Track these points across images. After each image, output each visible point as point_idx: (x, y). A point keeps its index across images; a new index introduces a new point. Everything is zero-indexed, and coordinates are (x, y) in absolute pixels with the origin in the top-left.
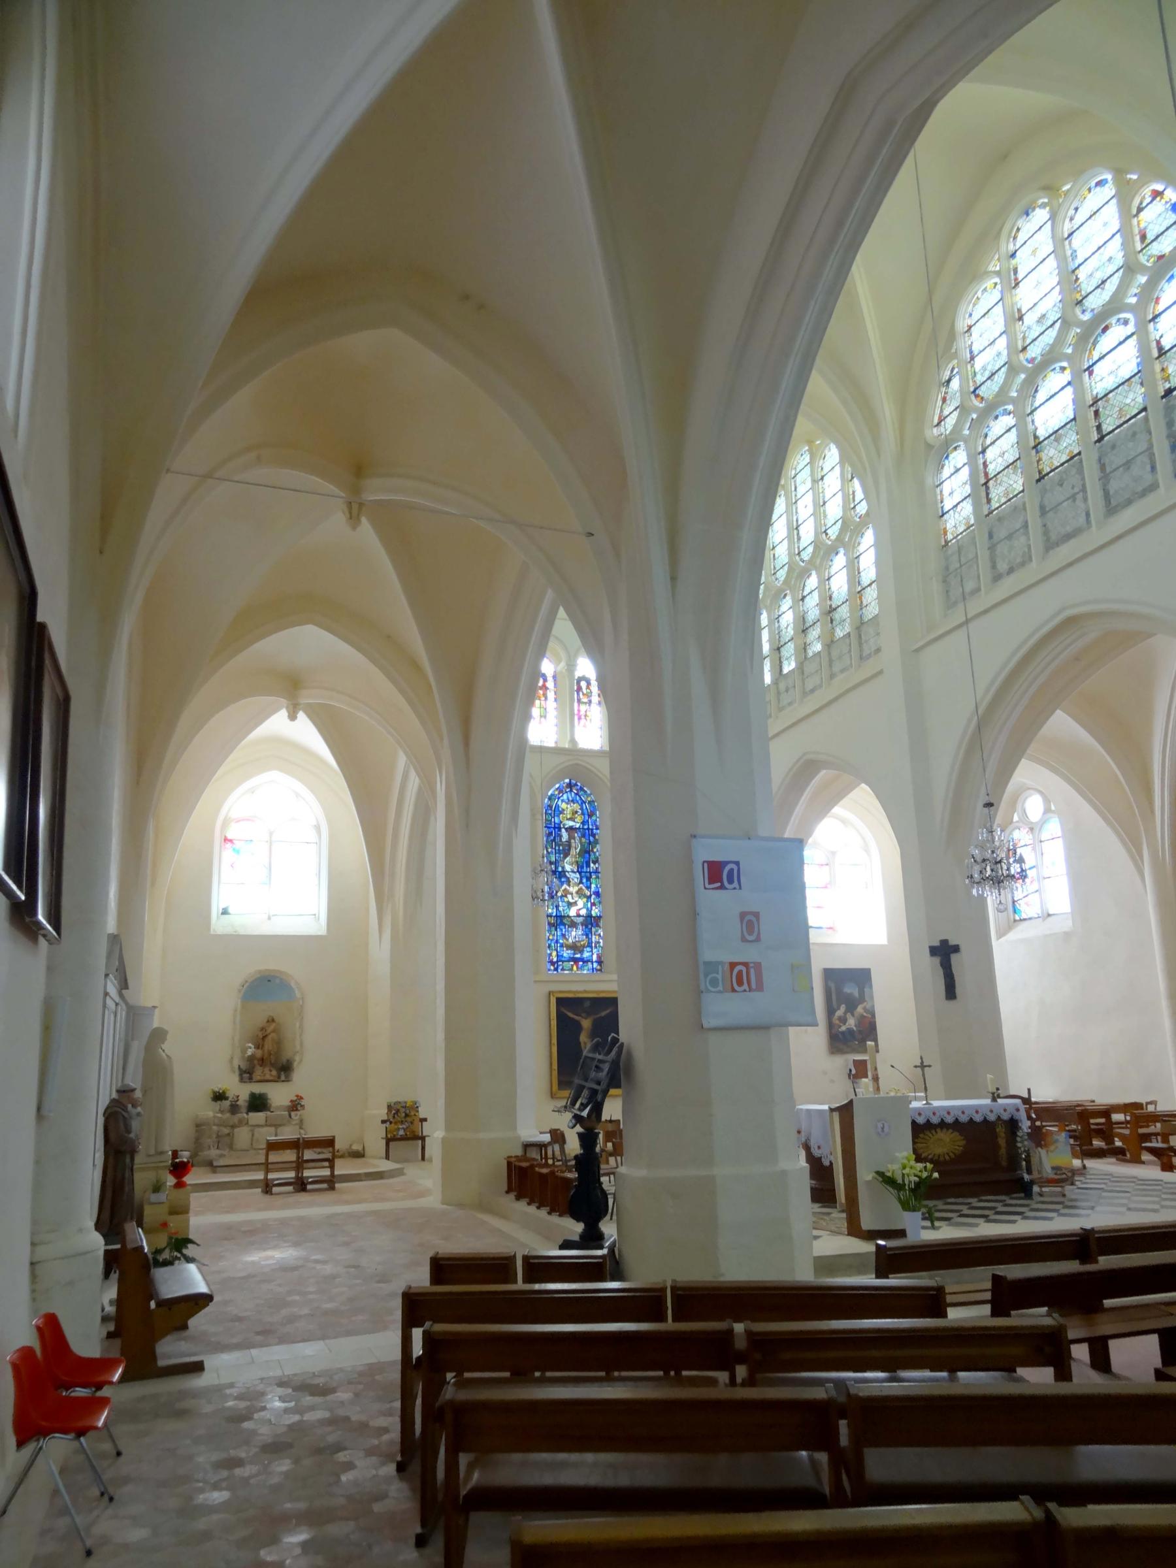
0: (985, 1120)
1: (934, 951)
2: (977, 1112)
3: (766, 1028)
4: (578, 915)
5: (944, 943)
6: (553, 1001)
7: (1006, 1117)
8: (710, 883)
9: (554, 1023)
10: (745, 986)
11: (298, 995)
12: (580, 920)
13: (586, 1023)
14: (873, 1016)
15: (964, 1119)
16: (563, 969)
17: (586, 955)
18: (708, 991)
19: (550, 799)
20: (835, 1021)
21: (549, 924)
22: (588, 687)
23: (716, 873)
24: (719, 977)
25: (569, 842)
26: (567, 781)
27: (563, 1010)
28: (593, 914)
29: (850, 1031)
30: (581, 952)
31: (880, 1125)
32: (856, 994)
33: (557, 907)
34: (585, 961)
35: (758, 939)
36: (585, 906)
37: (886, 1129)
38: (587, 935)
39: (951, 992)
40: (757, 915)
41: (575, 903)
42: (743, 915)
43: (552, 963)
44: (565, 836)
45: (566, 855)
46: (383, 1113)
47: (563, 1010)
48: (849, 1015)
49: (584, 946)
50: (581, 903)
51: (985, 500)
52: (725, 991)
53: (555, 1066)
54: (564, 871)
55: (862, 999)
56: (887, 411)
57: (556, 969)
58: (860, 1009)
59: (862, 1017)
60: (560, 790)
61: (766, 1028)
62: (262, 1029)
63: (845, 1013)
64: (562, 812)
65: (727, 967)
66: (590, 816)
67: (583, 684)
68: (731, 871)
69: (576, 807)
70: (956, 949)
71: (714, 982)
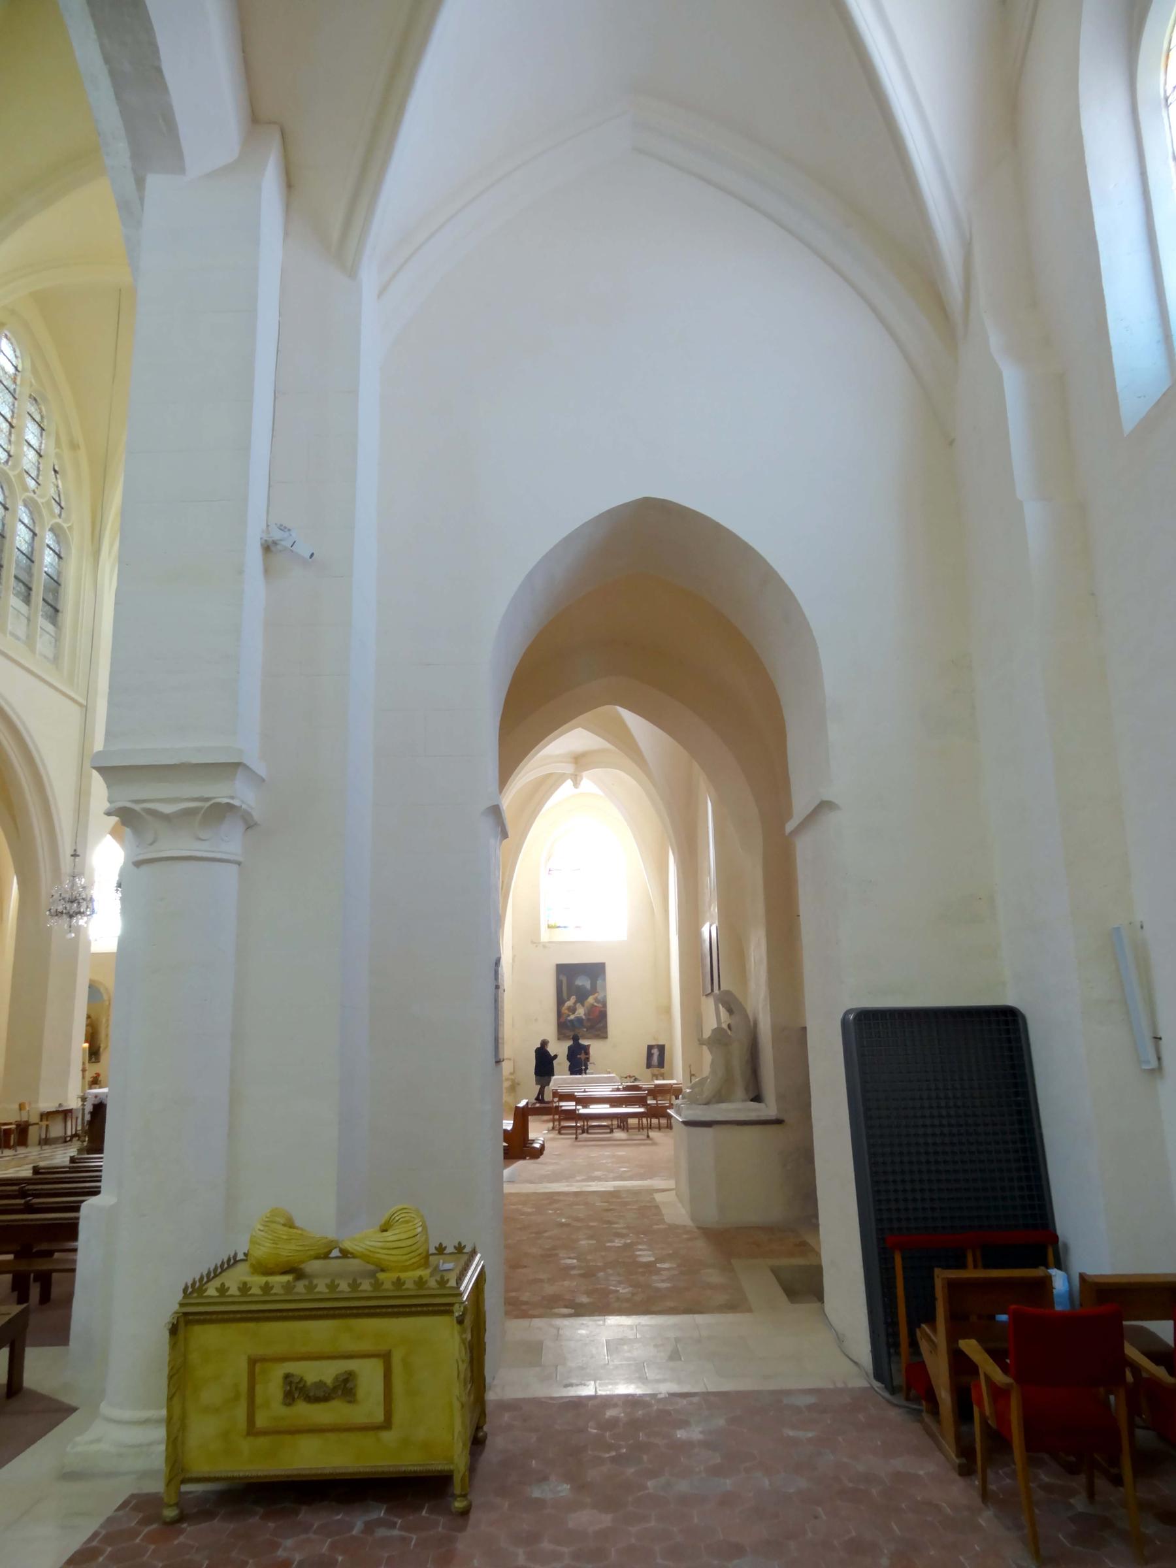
11: (105, 997)
14: (605, 1005)
20: (564, 1010)
29: (579, 1020)
32: (588, 986)
48: (578, 1005)
55: (594, 990)
58: (591, 1000)
59: (593, 1006)
63: (575, 1003)
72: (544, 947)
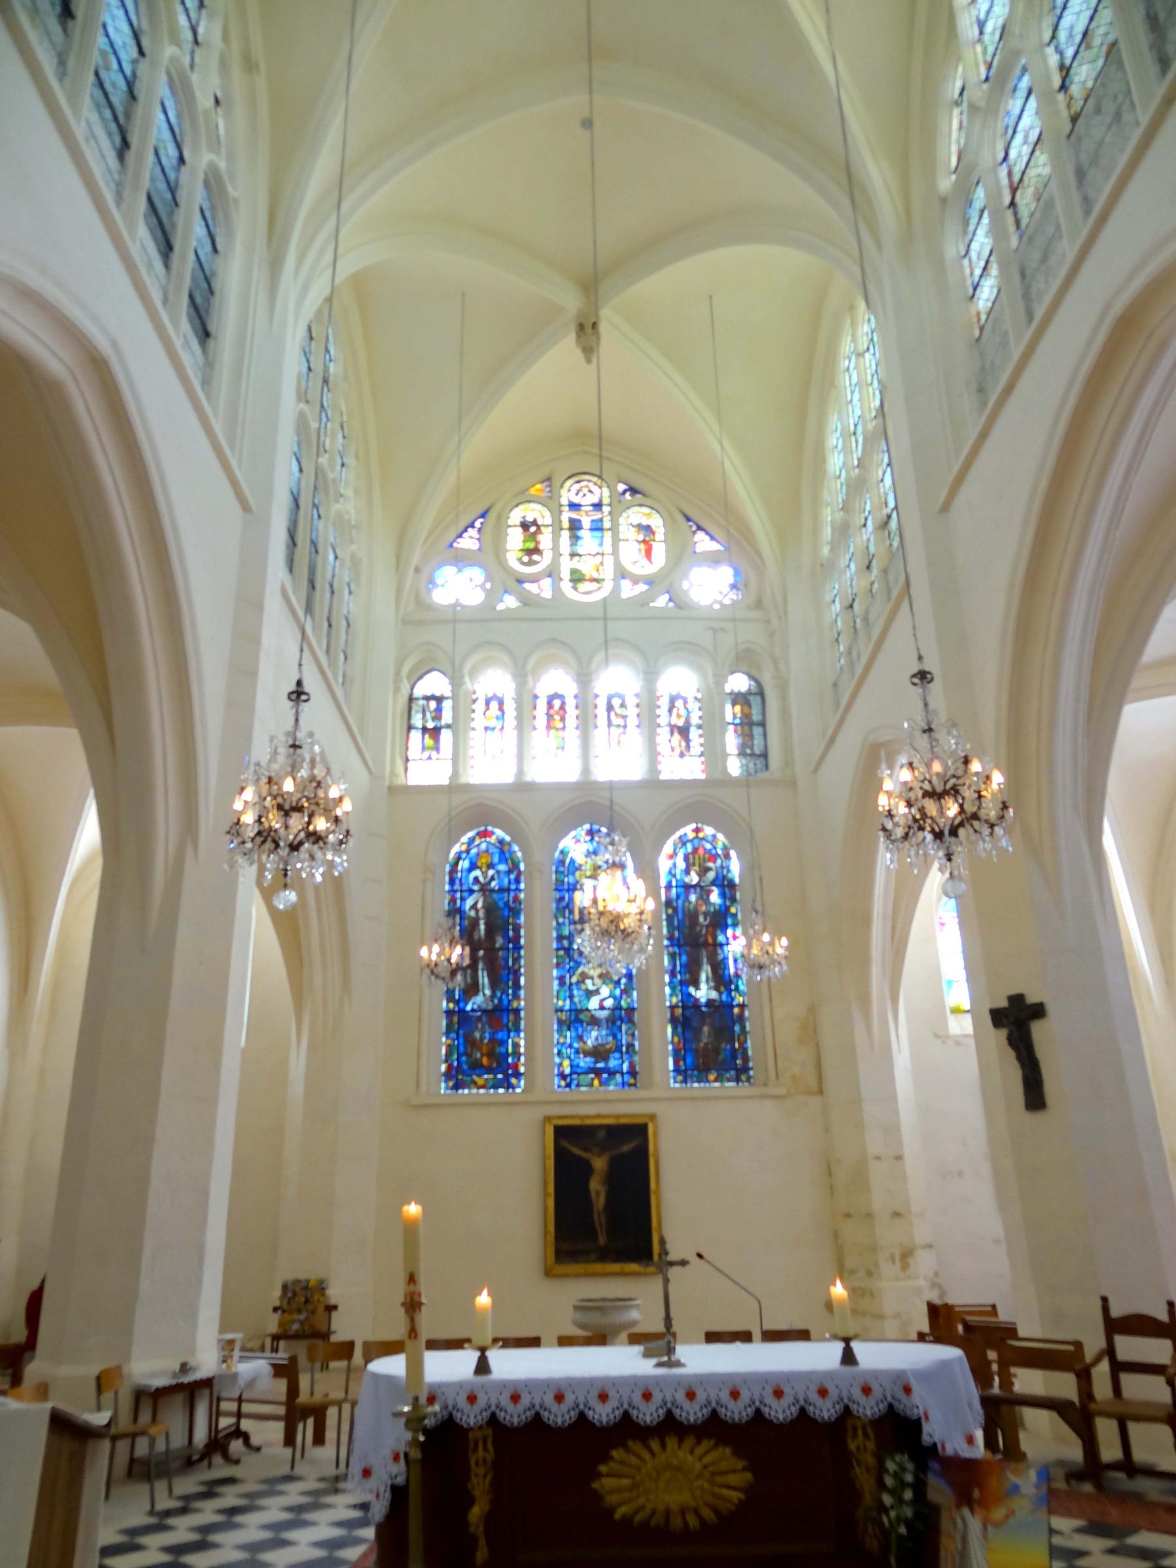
1: (998, 1017)
2: (778, 1393)
4: (602, 1008)
5: (1017, 1000)
6: (550, 1131)
7: (868, 1408)
9: (551, 1163)
12: (603, 1014)
13: (599, 1163)
15: (736, 1411)
16: (578, 1085)
17: (613, 1063)
22: (623, 705)
27: (565, 1144)
28: (623, 1003)
33: (571, 997)
34: (612, 1073)
36: (612, 996)
38: (615, 1037)
41: (597, 992)
43: (562, 1076)
46: (275, 1295)
47: (565, 1144)
50: (605, 991)
51: (1012, 228)
53: (551, 1228)
56: (877, 173)
57: (568, 1085)
67: (616, 702)
70: (1038, 1011)
72: (958, 1043)
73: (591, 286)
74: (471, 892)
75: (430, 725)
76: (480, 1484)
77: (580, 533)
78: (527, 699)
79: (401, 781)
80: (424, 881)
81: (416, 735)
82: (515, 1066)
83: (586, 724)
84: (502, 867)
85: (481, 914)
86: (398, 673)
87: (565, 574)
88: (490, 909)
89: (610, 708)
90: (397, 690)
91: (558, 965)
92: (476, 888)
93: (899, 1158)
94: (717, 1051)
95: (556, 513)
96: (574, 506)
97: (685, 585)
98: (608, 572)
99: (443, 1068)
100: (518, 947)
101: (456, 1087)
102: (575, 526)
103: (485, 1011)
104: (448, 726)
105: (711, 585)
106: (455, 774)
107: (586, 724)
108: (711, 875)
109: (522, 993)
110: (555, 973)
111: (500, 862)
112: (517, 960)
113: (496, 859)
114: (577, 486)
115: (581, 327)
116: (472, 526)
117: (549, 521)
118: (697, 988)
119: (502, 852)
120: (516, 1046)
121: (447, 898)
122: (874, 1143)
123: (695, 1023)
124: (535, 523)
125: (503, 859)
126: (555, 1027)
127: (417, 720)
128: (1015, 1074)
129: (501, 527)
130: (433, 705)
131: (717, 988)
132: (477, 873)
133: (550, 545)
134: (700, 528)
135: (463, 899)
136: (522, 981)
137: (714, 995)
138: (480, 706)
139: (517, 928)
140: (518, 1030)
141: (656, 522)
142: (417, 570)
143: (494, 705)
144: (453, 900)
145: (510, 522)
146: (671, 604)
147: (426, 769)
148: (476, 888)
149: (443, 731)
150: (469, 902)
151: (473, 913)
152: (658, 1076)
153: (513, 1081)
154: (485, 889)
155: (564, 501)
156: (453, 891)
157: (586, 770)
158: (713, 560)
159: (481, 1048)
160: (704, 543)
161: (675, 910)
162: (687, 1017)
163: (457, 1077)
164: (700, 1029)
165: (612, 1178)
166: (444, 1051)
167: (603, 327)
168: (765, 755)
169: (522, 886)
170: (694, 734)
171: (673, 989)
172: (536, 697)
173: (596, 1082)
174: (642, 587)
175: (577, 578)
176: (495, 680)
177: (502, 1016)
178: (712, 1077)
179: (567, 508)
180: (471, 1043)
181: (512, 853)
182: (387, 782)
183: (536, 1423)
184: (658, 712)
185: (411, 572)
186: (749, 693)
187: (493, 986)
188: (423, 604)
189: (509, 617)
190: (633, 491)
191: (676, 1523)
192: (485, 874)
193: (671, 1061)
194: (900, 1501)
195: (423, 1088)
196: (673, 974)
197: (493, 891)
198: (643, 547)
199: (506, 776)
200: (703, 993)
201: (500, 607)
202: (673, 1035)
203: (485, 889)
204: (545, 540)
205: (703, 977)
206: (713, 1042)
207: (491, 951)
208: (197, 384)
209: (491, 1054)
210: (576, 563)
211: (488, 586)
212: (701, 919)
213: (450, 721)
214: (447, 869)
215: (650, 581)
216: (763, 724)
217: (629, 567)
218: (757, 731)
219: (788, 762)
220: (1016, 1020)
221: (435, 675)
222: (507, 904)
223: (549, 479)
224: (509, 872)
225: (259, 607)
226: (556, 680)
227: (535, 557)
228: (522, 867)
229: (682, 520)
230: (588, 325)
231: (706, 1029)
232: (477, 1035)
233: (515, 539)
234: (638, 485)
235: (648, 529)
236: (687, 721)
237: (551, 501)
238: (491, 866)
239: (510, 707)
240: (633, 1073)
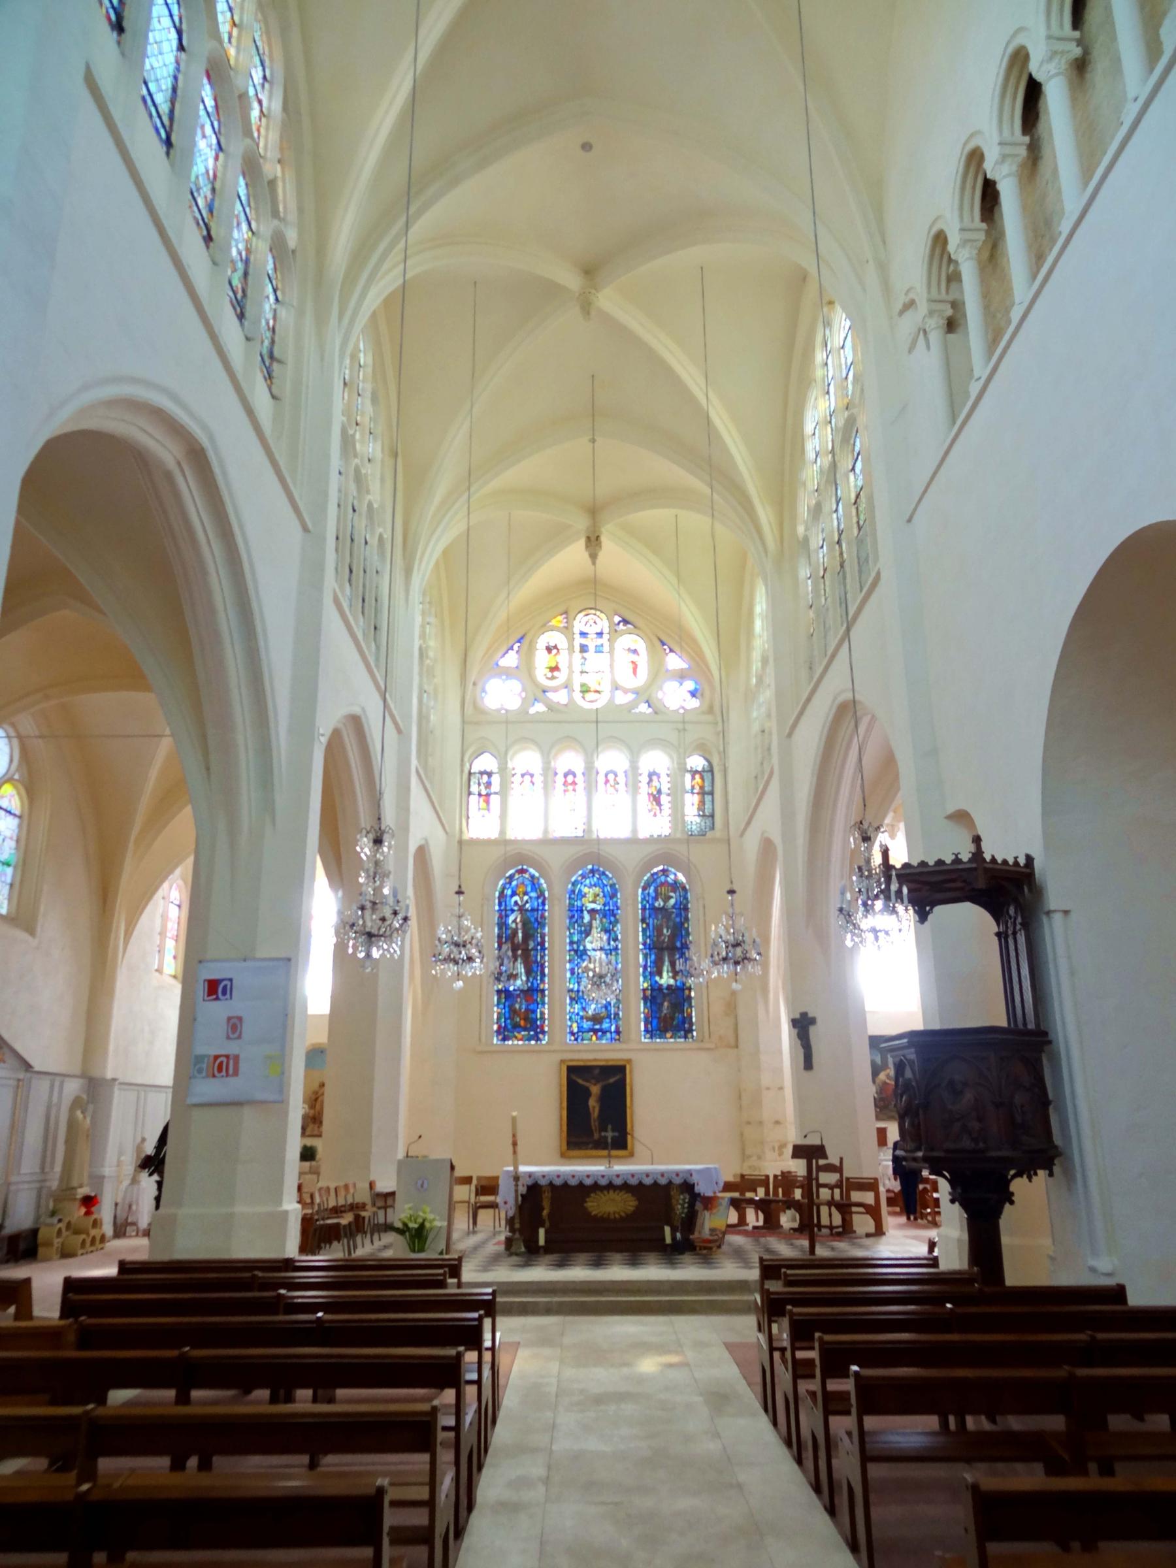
0: (656, 1184)
3: (238, 1104)
5: (804, 1015)
7: (678, 1181)
8: (209, 995)
9: (565, 1088)
10: (224, 1073)
13: (595, 1090)
15: (633, 1182)
17: (605, 1025)
18: (195, 1077)
19: (573, 884)
21: (572, 999)
23: (214, 988)
24: (205, 1066)
25: (590, 924)
26: (590, 867)
30: (601, 1023)
31: (420, 1182)
34: (604, 1032)
35: (239, 1037)
37: (425, 1185)
39: (808, 1064)
40: (240, 1019)
42: (229, 1019)
43: (572, 1034)
44: (587, 918)
45: (588, 933)
49: (604, 1018)
52: (207, 1076)
53: (565, 1128)
54: (585, 950)
56: (765, 515)
59: (885, 1083)
60: (583, 876)
61: (238, 1104)
62: (316, 1093)
64: (584, 896)
65: (212, 1059)
66: (611, 898)
67: (611, 777)
68: (225, 988)
69: (597, 890)
70: (813, 1021)
71: (200, 1071)
73: (594, 512)
74: (513, 911)
75: (484, 792)
76: (546, 1204)
77: (585, 655)
78: (551, 774)
79: (466, 836)
80: (482, 906)
81: (474, 799)
82: (542, 1026)
83: (590, 789)
84: (533, 894)
85: (520, 926)
86: (462, 760)
87: (577, 688)
88: (525, 923)
89: (607, 781)
90: (462, 771)
91: (570, 961)
92: (516, 908)
93: (781, 1088)
94: (673, 1019)
95: (571, 640)
96: (583, 634)
97: (660, 695)
98: (606, 687)
99: (495, 1027)
100: (543, 949)
101: (504, 1039)
102: (584, 649)
103: (522, 991)
104: (496, 793)
105: (677, 697)
106: (503, 832)
107: (590, 789)
108: (672, 901)
109: (546, 979)
110: (568, 966)
111: (532, 890)
112: (542, 957)
113: (529, 889)
114: (586, 618)
115: (588, 538)
116: (512, 648)
117: (566, 646)
118: (661, 977)
119: (533, 884)
120: (542, 1014)
121: (497, 915)
122: (766, 1079)
123: (659, 1001)
124: (555, 647)
125: (534, 889)
126: (568, 1001)
127: (474, 788)
128: (801, 1052)
129: (531, 649)
130: (485, 778)
131: (674, 977)
132: (516, 898)
133: (567, 665)
134: (671, 650)
135: (507, 916)
136: (546, 971)
137: (672, 982)
138: (517, 779)
139: (543, 937)
140: (543, 1004)
141: (639, 644)
142: (474, 684)
143: (527, 778)
144: (500, 917)
145: (538, 646)
146: (650, 710)
147: (481, 825)
148: (516, 908)
149: (492, 797)
150: (511, 918)
151: (514, 926)
152: (633, 1036)
153: (541, 1036)
154: (522, 909)
155: (576, 631)
156: (500, 910)
157: (589, 822)
158: (681, 676)
159: (521, 1017)
160: (675, 662)
161: (648, 925)
162: (654, 996)
163: (504, 1033)
164: (662, 1004)
165: (603, 1099)
166: (495, 1016)
167: (603, 539)
168: (712, 816)
169: (547, 907)
170: (664, 799)
171: (645, 977)
172: (556, 774)
173: (594, 1038)
174: (631, 696)
175: (585, 690)
176: (527, 759)
177: (532, 993)
178: (668, 1035)
179: (577, 636)
180: (513, 1012)
181: (540, 885)
182: (457, 838)
183: (565, 1185)
184: (640, 778)
185: (471, 686)
186: (704, 771)
187: (528, 972)
188: (479, 710)
189: (538, 719)
190: (625, 622)
191: (612, 1217)
192: (522, 899)
193: (642, 1024)
194: (683, 1208)
195: (483, 1040)
196: (645, 967)
197: (527, 910)
198: (631, 666)
199: (535, 834)
200: (666, 979)
201: (532, 711)
202: (645, 1007)
203: (522, 909)
204: (562, 659)
205: (665, 968)
206: (670, 1013)
207: (526, 952)
208: (373, 664)
209: (526, 1019)
210: (585, 679)
211: (524, 695)
212: (665, 931)
213: (497, 790)
214: (497, 894)
215: (636, 692)
216: (712, 793)
217: (621, 683)
218: (708, 798)
219: (727, 824)
220: (803, 1025)
221: (486, 754)
222: (536, 919)
223: (566, 613)
224: (538, 898)
225: (408, 789)
226: (570, 760)
227: (556, 674)
228: (547, 894)
229: (658, 644)
230: (593, 539)
231: (666, 1004)
232: (517, 1006)
233: (542, 661)
234: (629, 617)
235: (635, 651)
236: (659, 792)
237: (567, 630)
238: (526, 893)
239: (538, 779)
240: (618, 1032)
